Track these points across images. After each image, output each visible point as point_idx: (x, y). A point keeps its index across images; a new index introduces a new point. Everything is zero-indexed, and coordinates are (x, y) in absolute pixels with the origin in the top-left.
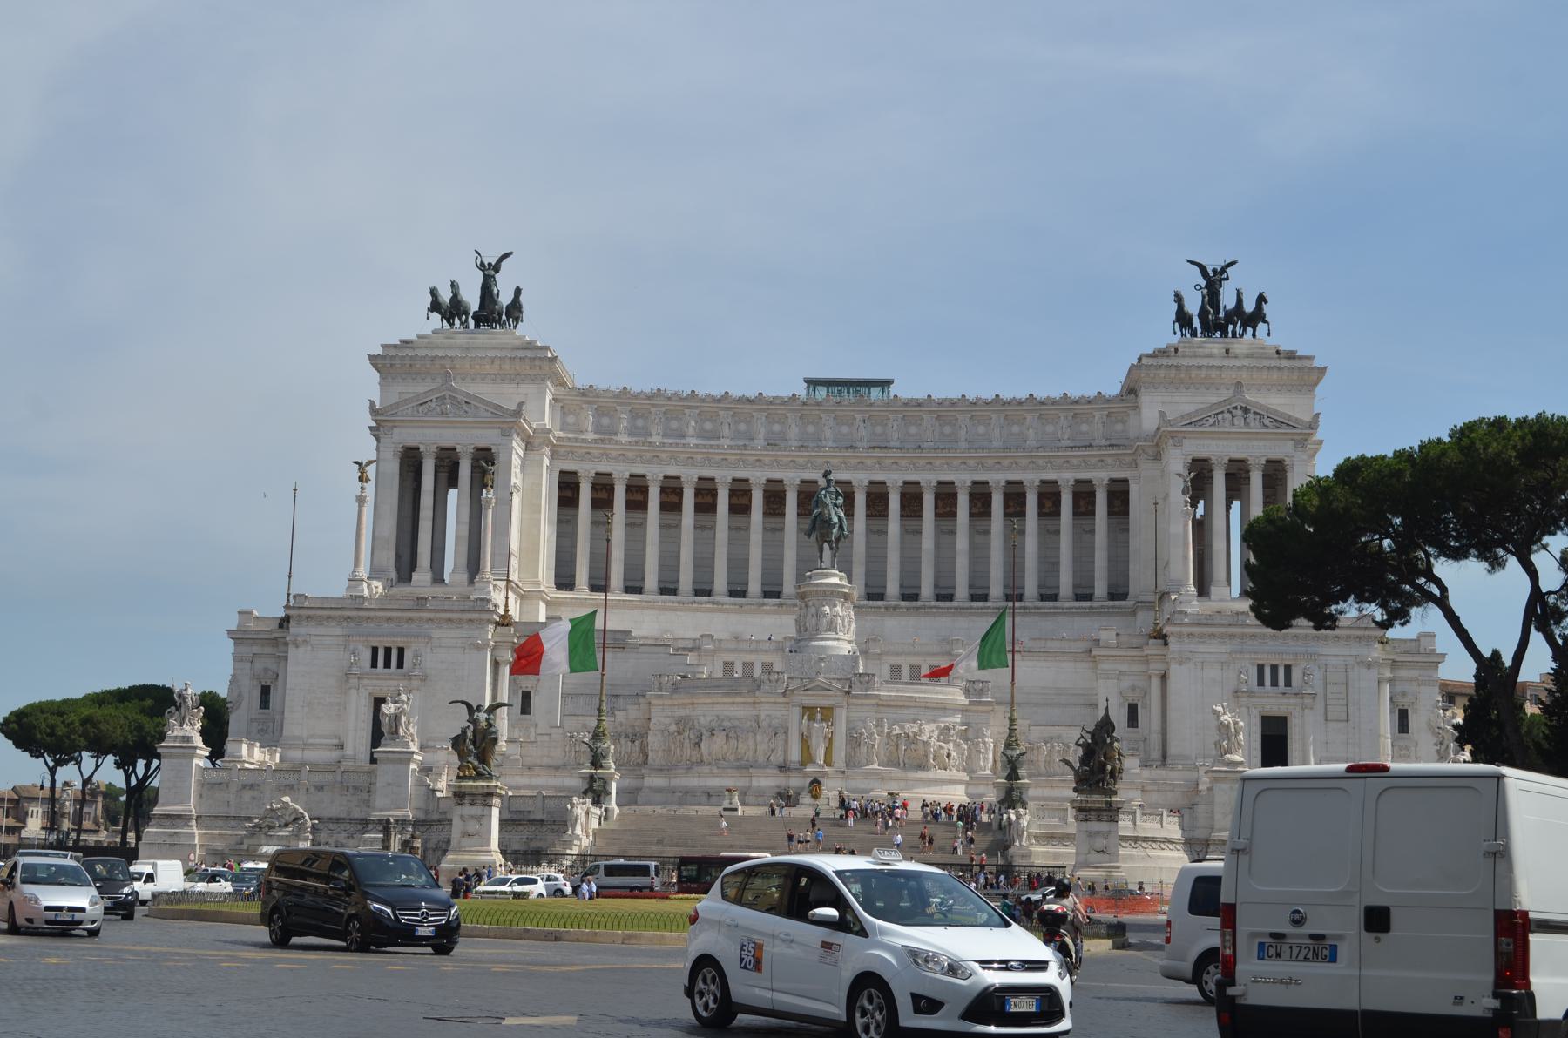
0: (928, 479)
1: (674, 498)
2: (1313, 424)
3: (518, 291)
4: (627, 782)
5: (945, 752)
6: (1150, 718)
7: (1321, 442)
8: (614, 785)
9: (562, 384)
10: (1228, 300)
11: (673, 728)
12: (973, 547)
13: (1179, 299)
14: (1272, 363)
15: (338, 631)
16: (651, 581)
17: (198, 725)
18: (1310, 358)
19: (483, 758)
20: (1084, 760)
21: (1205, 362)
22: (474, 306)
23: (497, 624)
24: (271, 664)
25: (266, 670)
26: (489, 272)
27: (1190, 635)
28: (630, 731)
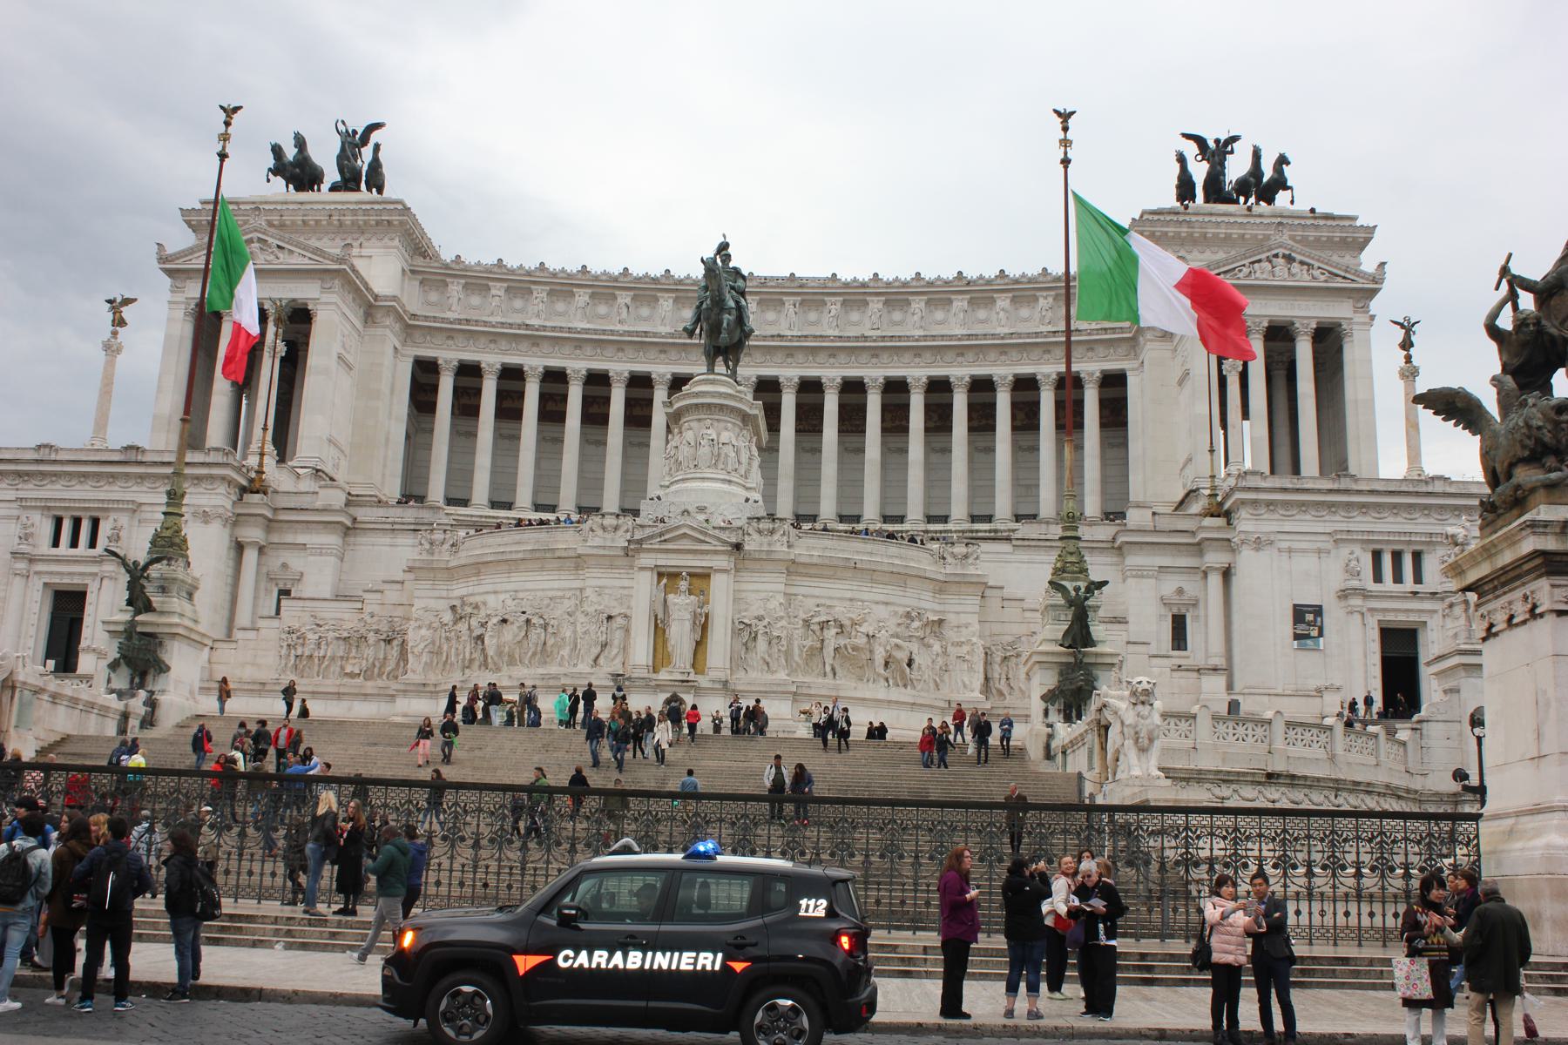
0: (874, 373)
2: (1377, 279)
3: (377, 147)
5: (902, 656)
6: (1205, 638)
9: (424, 255)
10: (1236, 168)
11: (448, 617)
13: (1181, 159)
14: (1309, 222)
15: (11, 495)
18: (1354, 218)
22: (332, 175)
23: (243, 490)
27: (1269, 504)
28: (384, 627)
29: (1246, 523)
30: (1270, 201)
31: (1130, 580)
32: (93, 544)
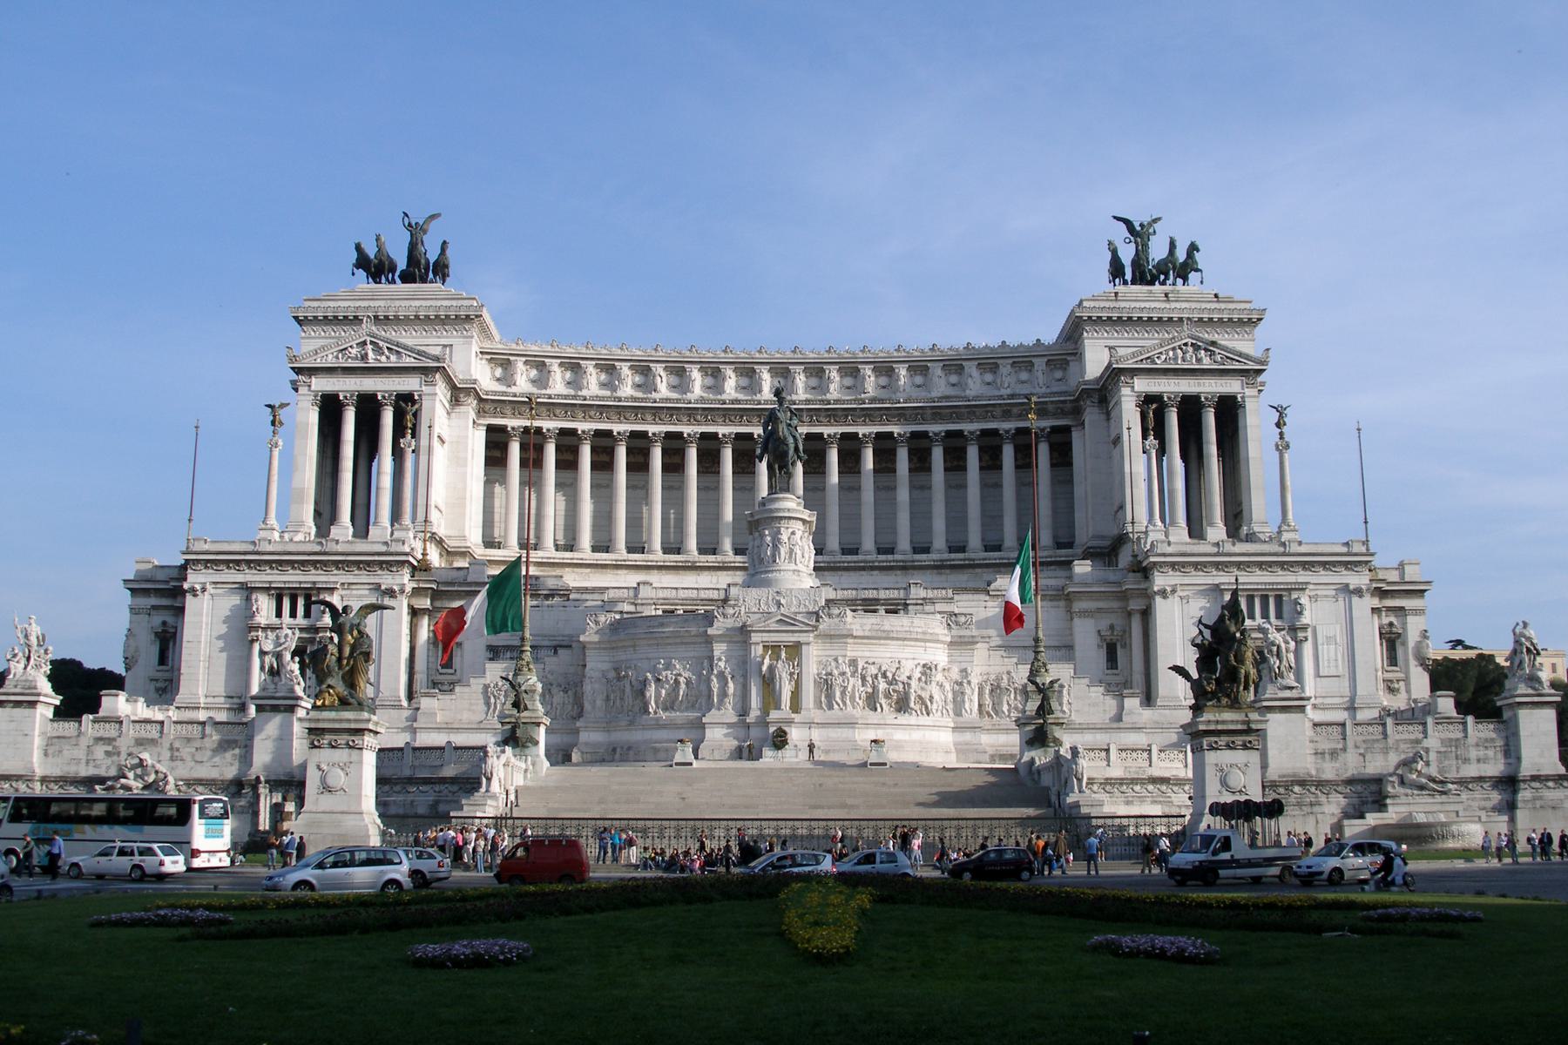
1: (604, 458)
4: (557, 739)
7: (1263, 384)
8: (542, 729)
10: (1158, 251)
11: (612, 674)
12: (912, 503)
14: (1213, 306)
16: (586, 539)
17: (47, 668)
19: (351, 681)
20: (1205, 662)
21: (1143, 305)
22: (402, 264)
24: (170, 620)
25: (164, 623)
26: (416, 232)
29: (1160, 581)
30: (1185, 279)
31: (1076, 621)
32: (307, 614)
